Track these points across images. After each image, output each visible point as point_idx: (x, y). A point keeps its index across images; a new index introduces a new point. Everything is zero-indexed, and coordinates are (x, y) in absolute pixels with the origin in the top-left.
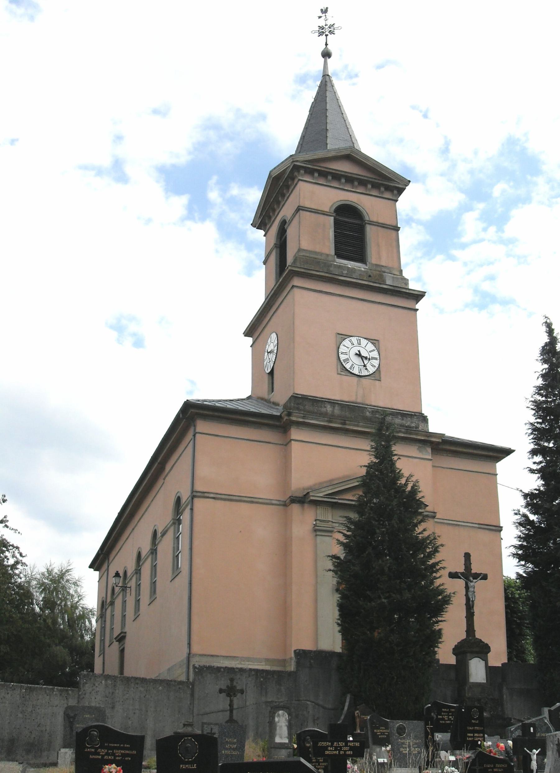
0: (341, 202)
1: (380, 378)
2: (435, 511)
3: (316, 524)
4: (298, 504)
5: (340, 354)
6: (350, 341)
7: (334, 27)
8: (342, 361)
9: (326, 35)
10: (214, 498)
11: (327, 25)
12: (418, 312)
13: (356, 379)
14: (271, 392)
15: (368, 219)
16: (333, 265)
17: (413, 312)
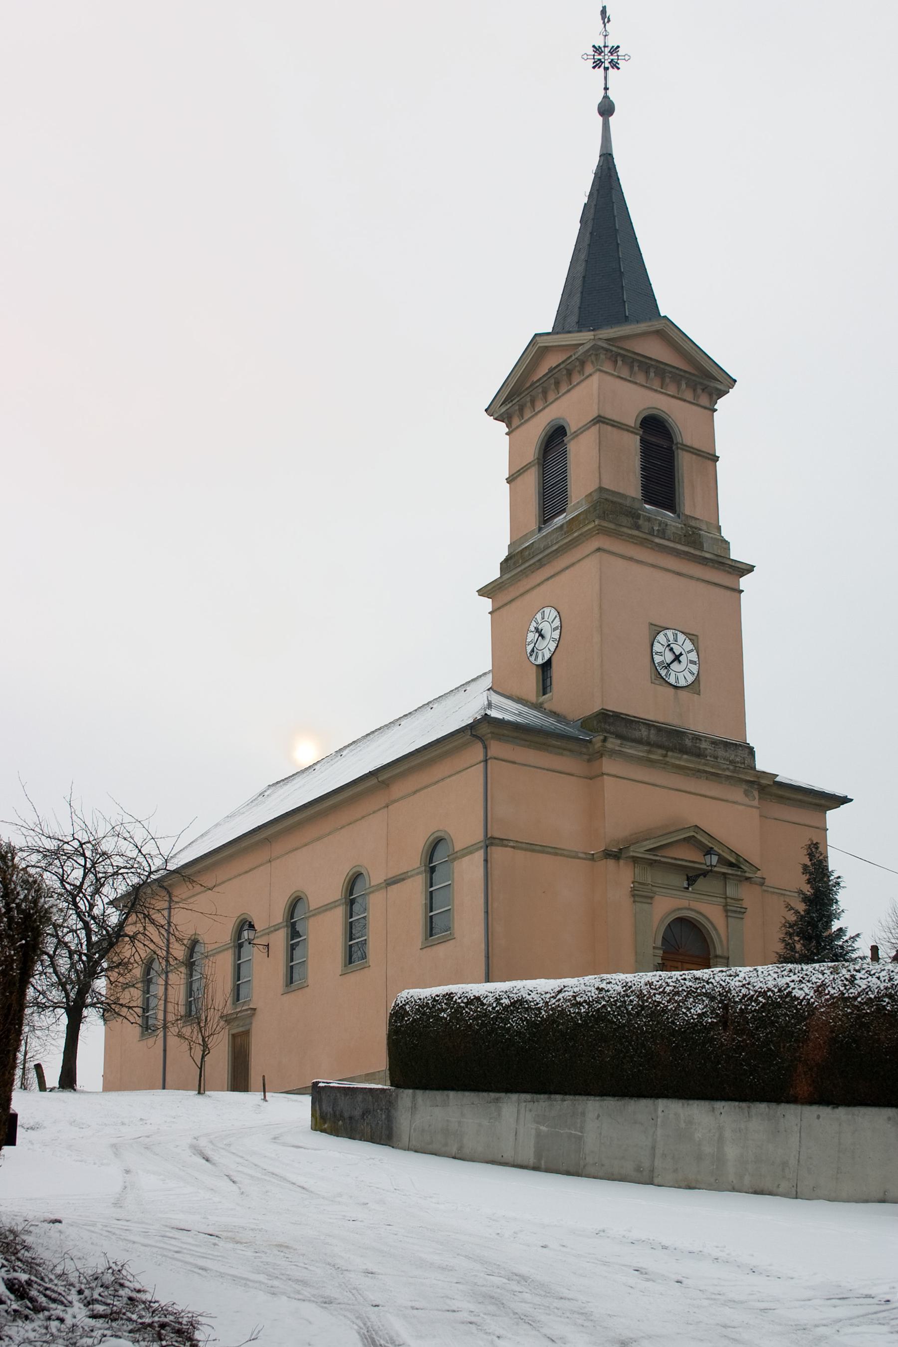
0: (649, 410)
1: (700, 692)
2: (764, 877)
3: (634, 887)
4: (613, 861)
5: (654, 654)
6: (666, 635)
7: (619, 53)
8: (657, 665)
9: (606, 69)
10: (513, 847)
11: (608, 46)
12: (742, 594)
13: (672, 690)
14: (541, 694)
15: (681, 442)
16: (641, 516)
17: (736, 594)
